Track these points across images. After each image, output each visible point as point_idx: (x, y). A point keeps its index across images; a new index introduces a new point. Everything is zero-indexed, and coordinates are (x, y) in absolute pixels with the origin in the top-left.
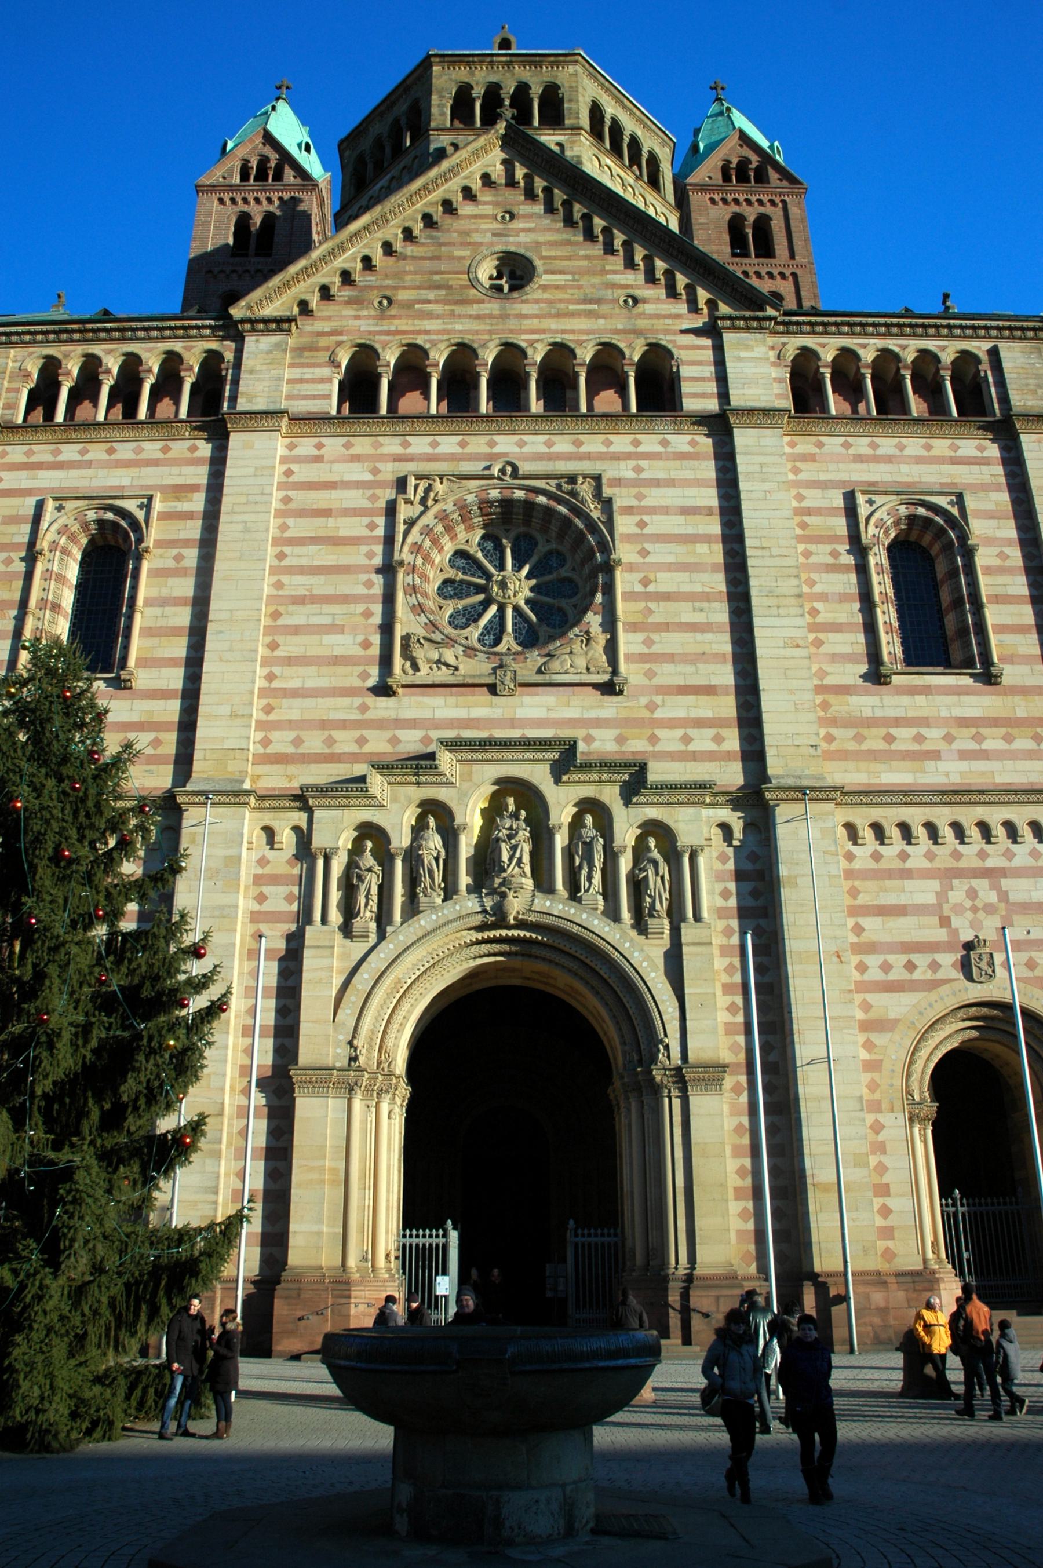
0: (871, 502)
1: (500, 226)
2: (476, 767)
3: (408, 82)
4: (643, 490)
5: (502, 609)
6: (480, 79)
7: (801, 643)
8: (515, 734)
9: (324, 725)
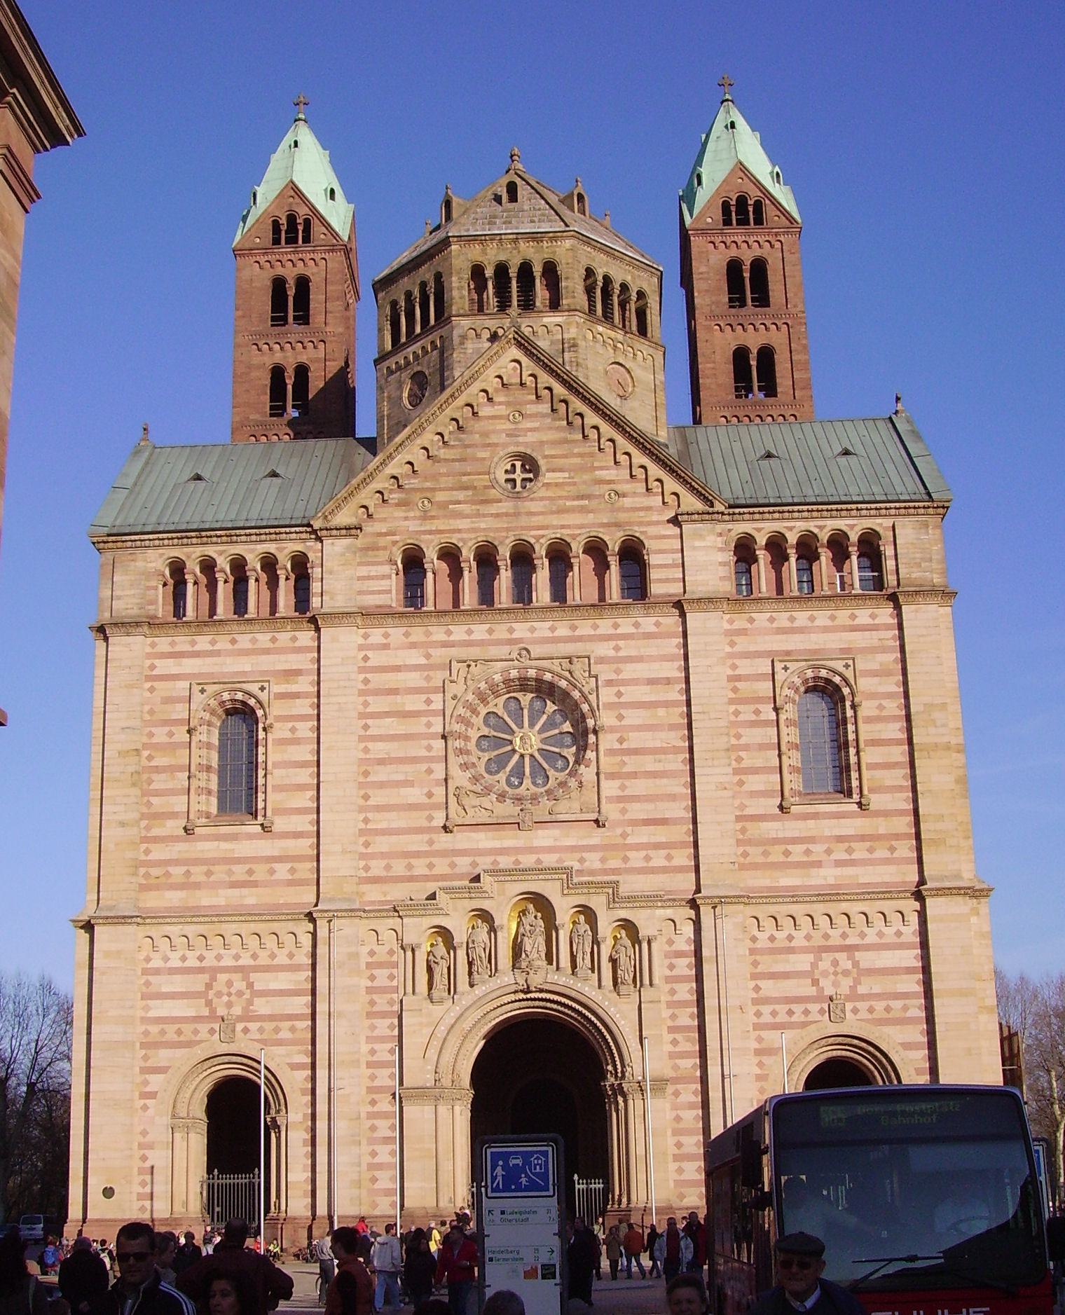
0: (786, 669)
1: (513, 427)
2: (507, 885)
3: (432, 251)
5: (522, 756)
6: (490, 257)
7: (727, 786)
9: (407, 855)
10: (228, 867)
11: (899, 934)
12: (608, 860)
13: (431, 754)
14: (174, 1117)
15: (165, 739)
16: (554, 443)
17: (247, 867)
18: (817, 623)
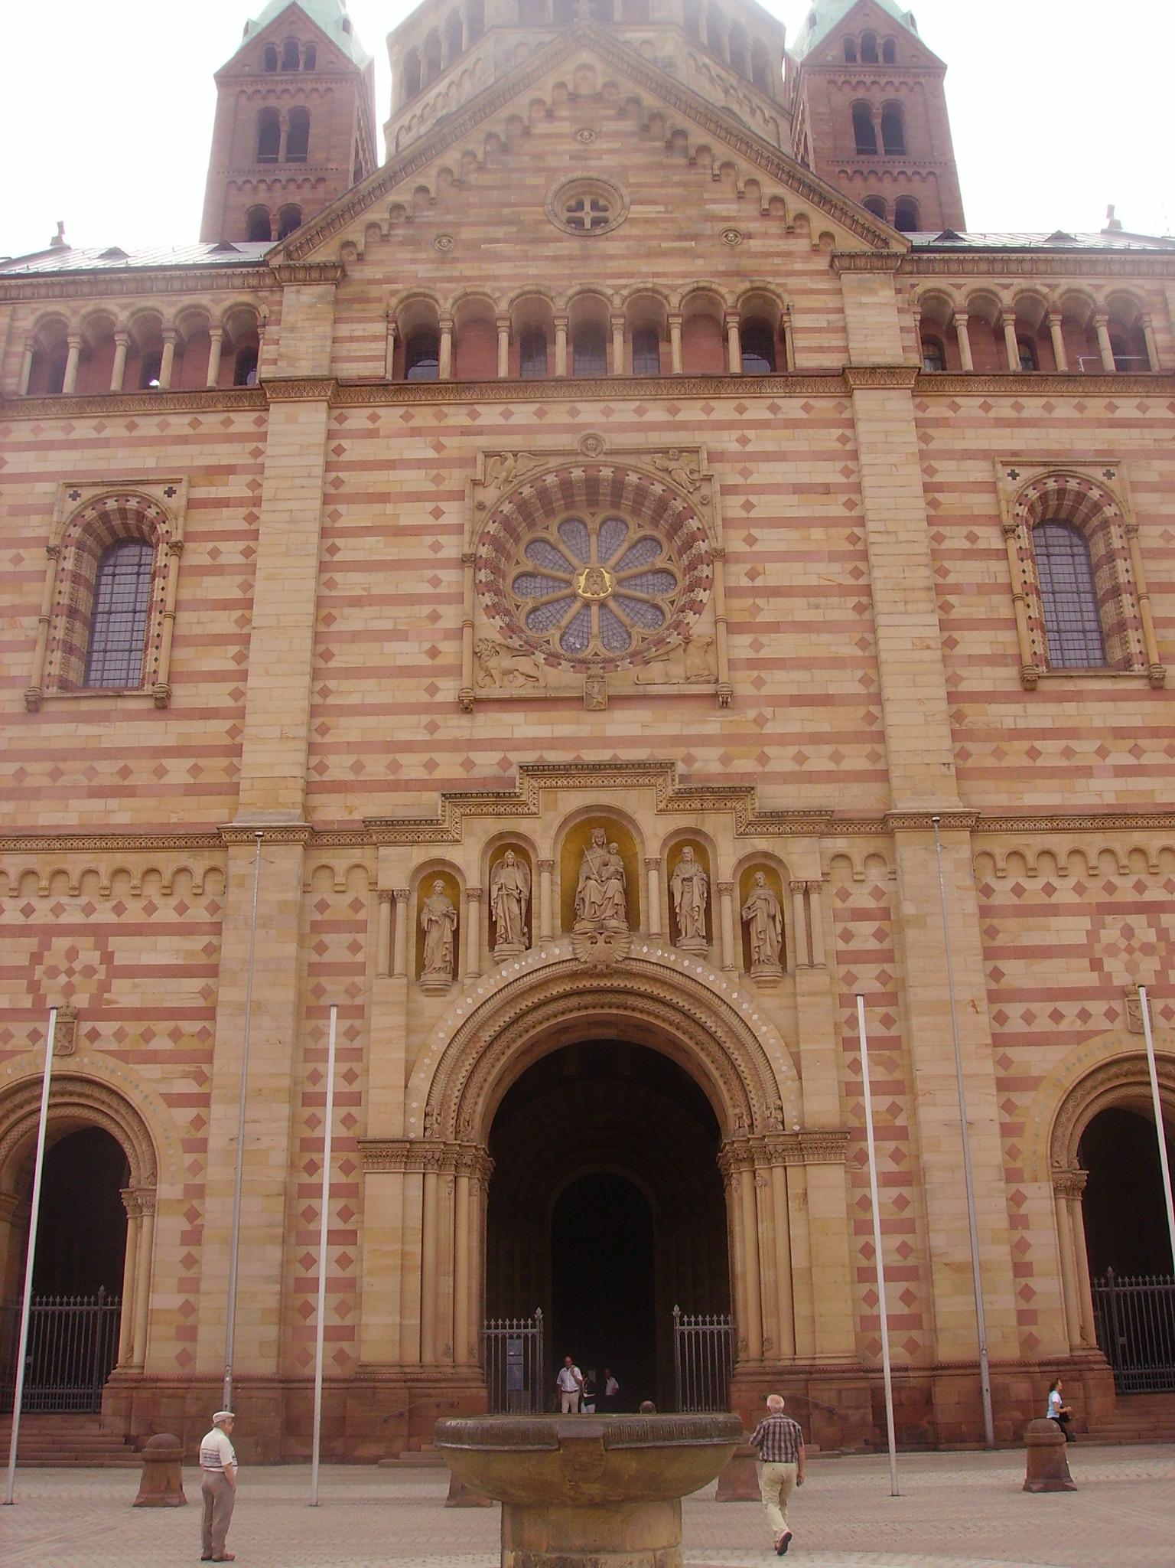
0: (1014, 475)
1: (581, 147)
2: (562, 795)
4: (751, 466)
7: (932, 644)
8: (604, 755)
10: (88, 764)
12: (733, 760)
13: (438, 590)
17: (121, 763)
18: (1058, 413)
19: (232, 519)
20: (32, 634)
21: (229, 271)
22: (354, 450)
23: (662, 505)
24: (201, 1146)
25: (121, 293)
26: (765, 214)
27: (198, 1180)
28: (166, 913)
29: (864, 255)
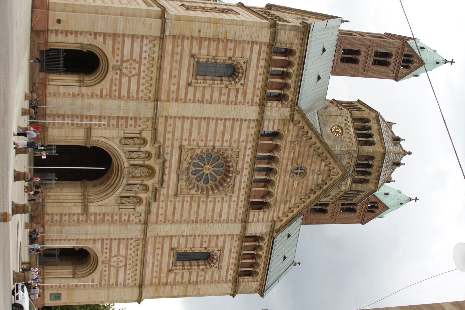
0: (218, 250)
1: (316, 171)
4: (228, 203)
6: (375, 163)
7: (183, 234)
10: (178, 68)
11: (129, 279)
14: (87, 44)
15: (229, 47)
16: (307, 185)
17: (177, 76)
19: (232, 97)
20: (211, 54)
21: (297, 96)
22: (245, 124)
23: (222, 185)
24: (92, 96)
25: (298, 70)
26: (290, 208)
27: (85, 96)
28: (141, 88)
29: (274, 228)
